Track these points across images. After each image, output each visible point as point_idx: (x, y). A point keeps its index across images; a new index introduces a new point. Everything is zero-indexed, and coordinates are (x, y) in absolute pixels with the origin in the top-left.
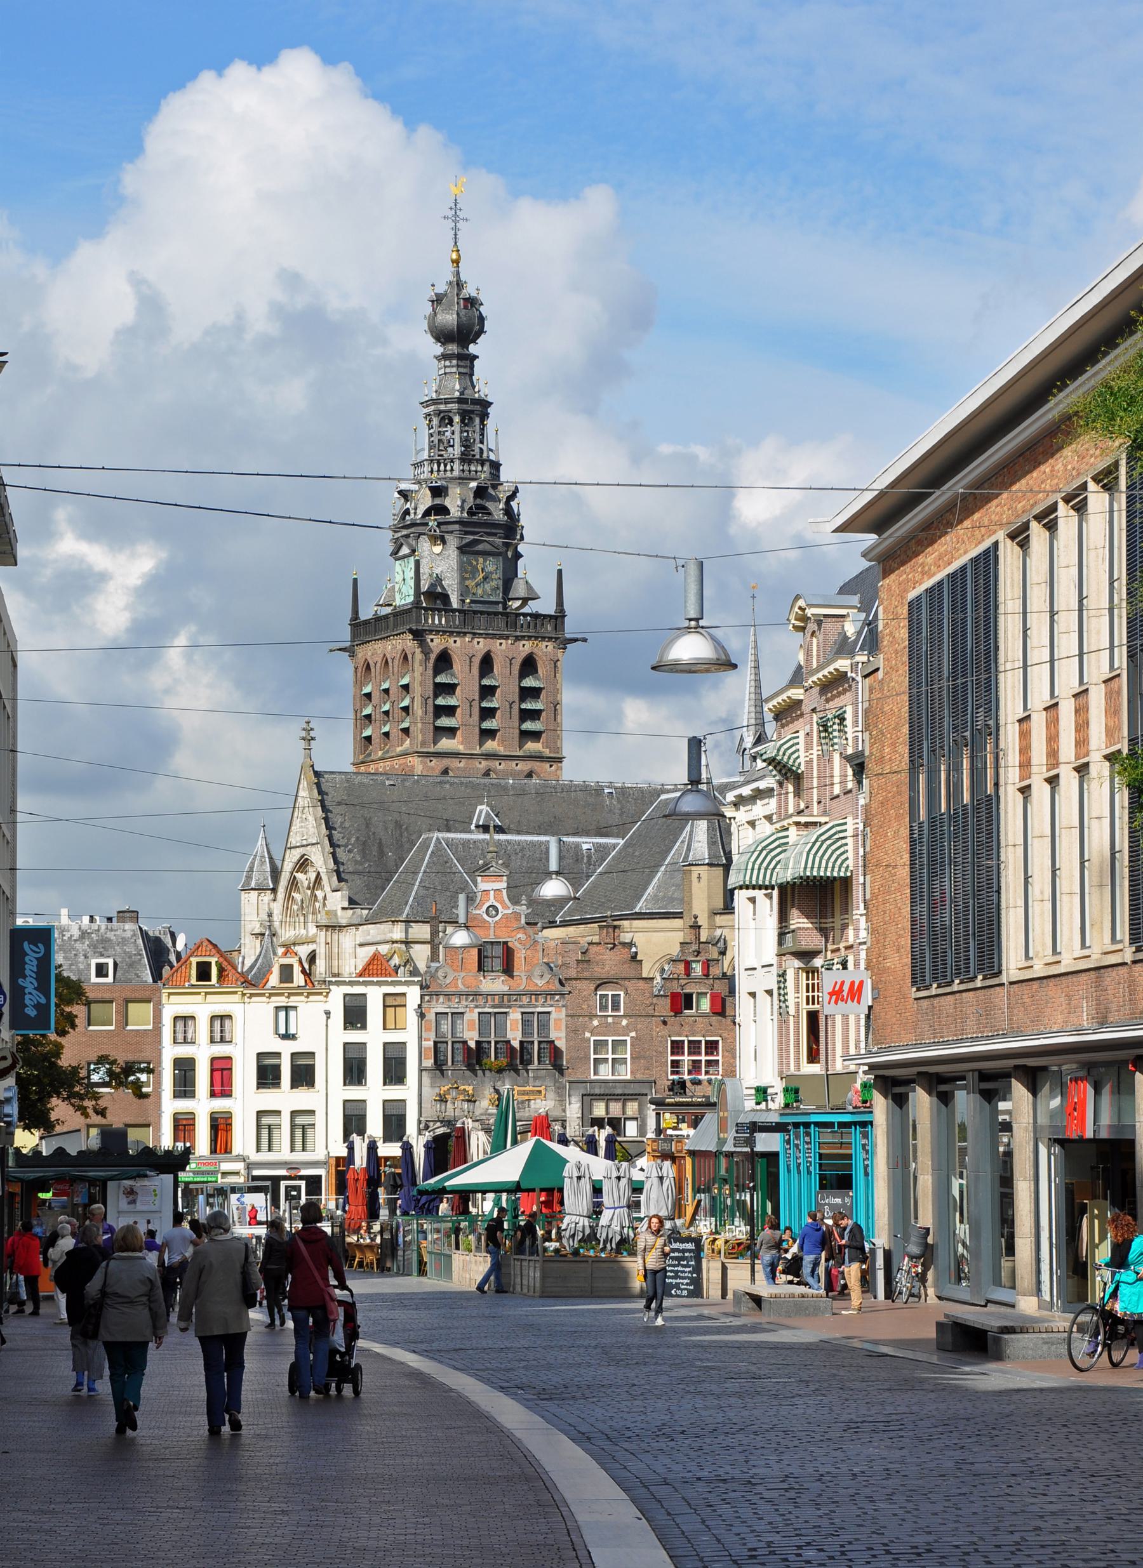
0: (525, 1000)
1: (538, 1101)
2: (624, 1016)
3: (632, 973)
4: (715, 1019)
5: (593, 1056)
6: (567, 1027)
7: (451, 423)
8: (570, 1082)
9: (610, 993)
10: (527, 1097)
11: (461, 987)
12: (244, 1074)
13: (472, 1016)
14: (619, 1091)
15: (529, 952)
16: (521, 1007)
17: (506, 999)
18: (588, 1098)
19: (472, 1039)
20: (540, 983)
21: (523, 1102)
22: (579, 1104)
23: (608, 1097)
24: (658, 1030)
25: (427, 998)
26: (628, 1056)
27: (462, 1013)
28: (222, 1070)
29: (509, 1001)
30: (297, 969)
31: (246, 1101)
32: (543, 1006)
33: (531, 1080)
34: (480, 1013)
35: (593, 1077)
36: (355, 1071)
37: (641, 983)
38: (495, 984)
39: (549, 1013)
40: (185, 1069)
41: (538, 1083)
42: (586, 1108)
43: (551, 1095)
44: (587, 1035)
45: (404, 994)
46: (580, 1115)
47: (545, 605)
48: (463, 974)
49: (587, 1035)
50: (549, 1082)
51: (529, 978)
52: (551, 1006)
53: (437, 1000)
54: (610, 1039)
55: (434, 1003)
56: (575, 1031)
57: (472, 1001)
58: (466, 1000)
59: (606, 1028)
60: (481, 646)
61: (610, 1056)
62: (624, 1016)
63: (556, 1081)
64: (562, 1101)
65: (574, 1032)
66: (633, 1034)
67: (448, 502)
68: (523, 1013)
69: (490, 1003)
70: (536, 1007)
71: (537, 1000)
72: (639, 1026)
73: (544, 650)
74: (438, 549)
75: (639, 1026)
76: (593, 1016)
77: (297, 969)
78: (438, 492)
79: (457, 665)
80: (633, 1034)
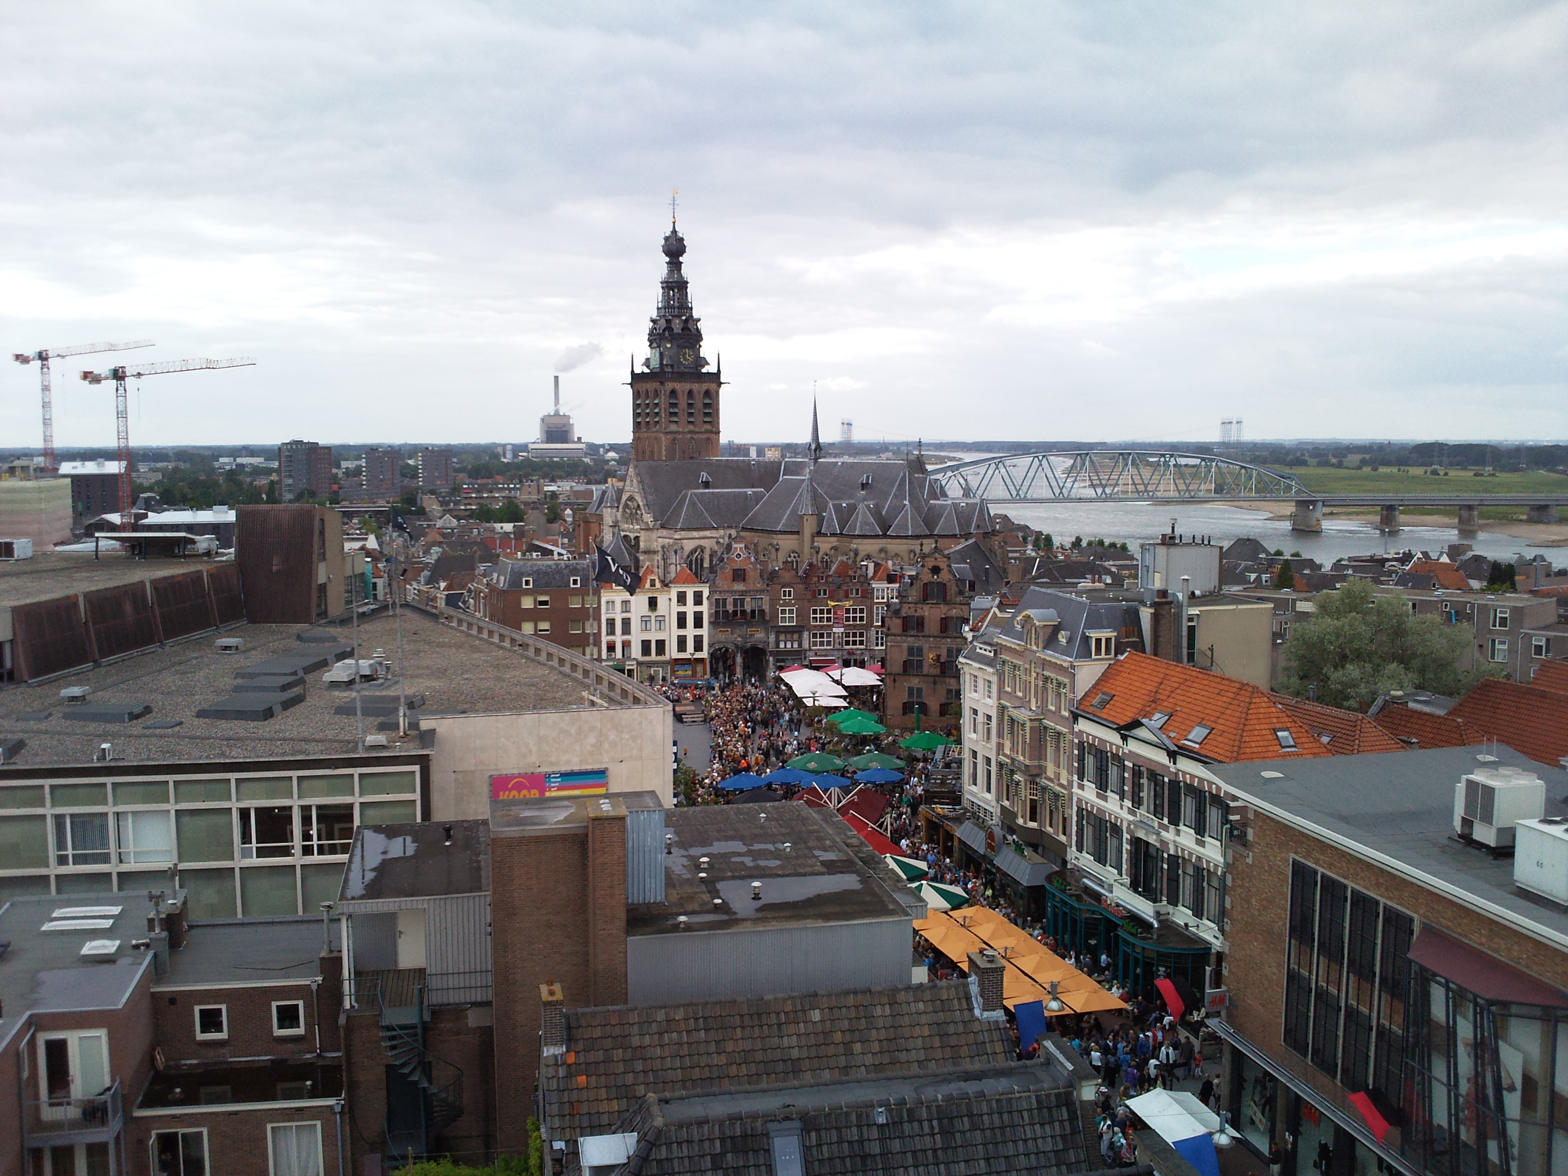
12: (635, 625)
13: (730, 600)
17: (743, 593)
23: (785, 632)
28: (626, 623)
30: (657, 581)
31: (636, 638)
36: (682, 622)
38: (739, 587)
40: (611, 623)
47: (711, 368)
60: (687, 386)
65: (773, 606)
73: (713, 386)
77: (657, 581)
78: (668, 321)
79: (680, 395)
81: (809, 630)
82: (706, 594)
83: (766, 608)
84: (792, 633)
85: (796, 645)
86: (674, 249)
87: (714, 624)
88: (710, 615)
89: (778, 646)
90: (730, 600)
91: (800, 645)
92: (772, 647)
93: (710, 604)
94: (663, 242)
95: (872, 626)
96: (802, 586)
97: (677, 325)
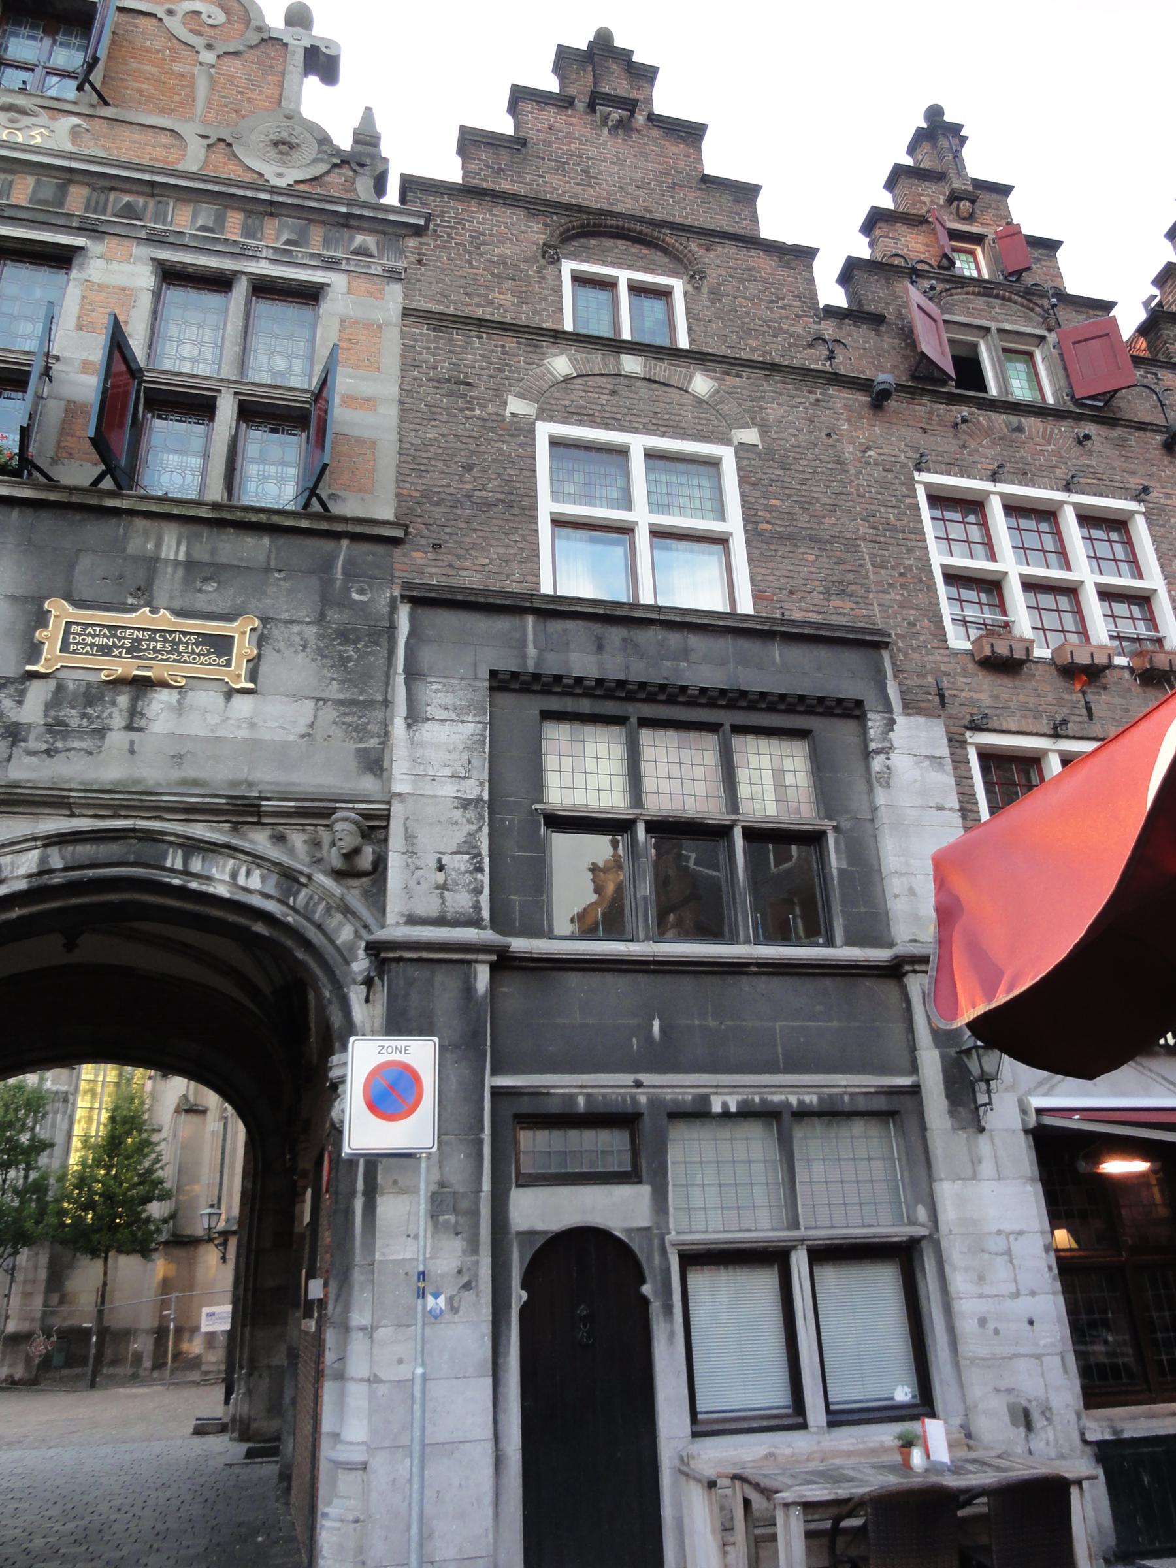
1: (206, 699)
5: (546, 507)
6: (408, 362)
8: (423, 600)
9: (624, 276)
15: (233, 66)
21: (94, 695)
22: (468, 729)
26: (734, 524)
32: (283, 256)
33: (168, 583)
41: (210, 596)
43: (295, 667)
46: (475, 789)
52: (331, 264)
54: (637, 443)
61: (642, 516)
62: (698, 358)
66: (750, 436)
70: (243, 253)
72: (774, 412)
80: (750, 436)
81: (934, 701)
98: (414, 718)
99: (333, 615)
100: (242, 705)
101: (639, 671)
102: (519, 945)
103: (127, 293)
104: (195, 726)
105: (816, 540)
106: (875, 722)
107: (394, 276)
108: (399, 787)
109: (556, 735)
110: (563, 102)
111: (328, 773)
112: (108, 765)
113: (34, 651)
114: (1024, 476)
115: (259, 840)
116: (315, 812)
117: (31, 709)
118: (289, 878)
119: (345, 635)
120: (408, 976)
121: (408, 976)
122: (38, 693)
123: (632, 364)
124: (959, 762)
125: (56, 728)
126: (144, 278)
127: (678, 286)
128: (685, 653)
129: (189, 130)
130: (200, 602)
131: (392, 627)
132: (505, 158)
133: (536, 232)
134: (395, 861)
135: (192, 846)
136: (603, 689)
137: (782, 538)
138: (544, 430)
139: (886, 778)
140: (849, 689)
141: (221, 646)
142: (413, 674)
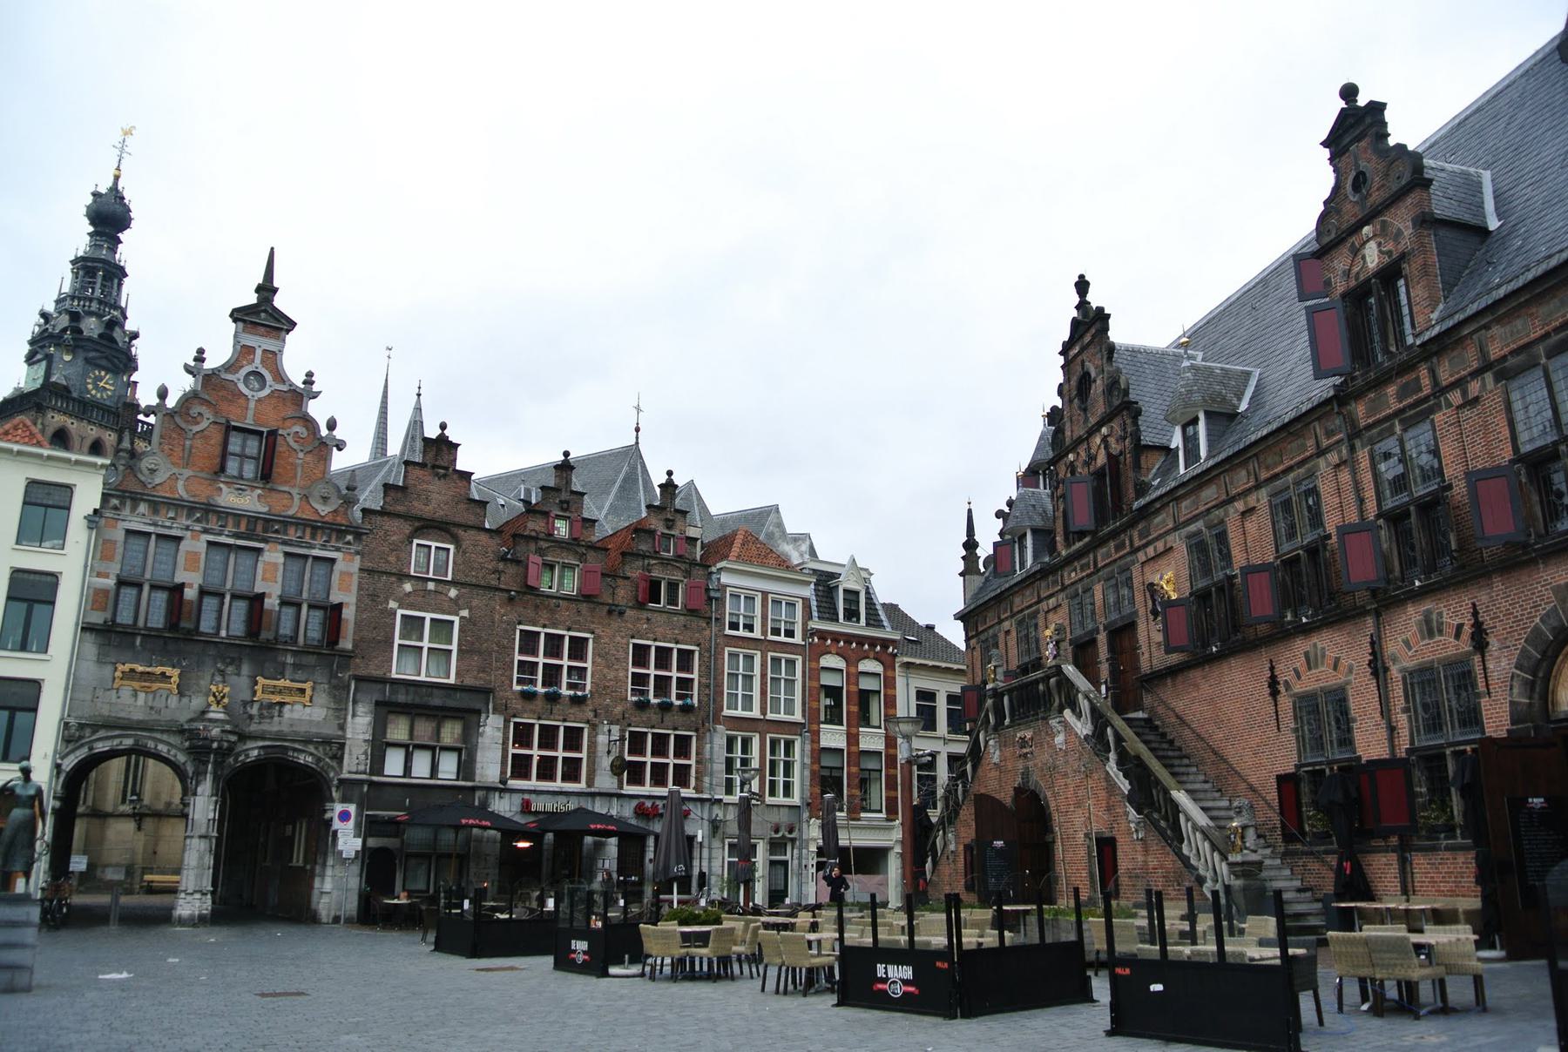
0: (292, 534)
1: (298, 707)
2: (453, 583)
3: (471, 519)
4: (584, 607)
5: (397, 641)
6: (360, 588)
7: (94, 276)
8: (359, 679)
9: (434, 544)
10: (277, 698)
11: (181, 491)
13: (195, 544)
14: (437, 702)
15: (309, 458)
16: (285, 543)
17: (260, 528)
18: (385, 710)
19: (191, 586)
20: (324, 510)
21: (271, 706)
24: (501, 612)
25: (115, 502)
26: (454, 647)
27: (178, 539)
29: (265, 530)
32: (323, 547)
33: (288, 673)
34: (210, 543)
35: (394, 675)
37: (483, 537)
39: (333, 561)
41: (300, 675)
42: (379, 727)
43: (322, 698)
44: (392, 604)
45: (68, 489)
46: (368, 737)
48: (188, 473)
49: (392, 604)
50: (320, 676)
51: (305, 498)
52: (338, 549)
53: (134, 509)
54: (428, 616)
55: (127, 511)
56: (373, 596)
57: (198, 520)
58: (189, 517)
59: (422, 598)
61: (426, 644)
62: (453, 583)
63: (333, 675)
64: (340, 713)
65: (371, 599)
66: (465, 613)
67: (83, 326)
68: (287, 554)
69: (230, 528)
70: (312, 547)
71: (313, 537)
72: (475, 603)
74: (67, 358)
75: (475, 603)
76: (404, 576)
78: (75, 317)
80: (465, 613)
81: (504, 710)
82: (88, 494)
83: (345, 595)
84: (440, 714)
85: (448, 767)
86: (109, 217)
87: (107, 634)
88: (95, 598)
89: (377, 764)
90: (195, 544)
91: (466, 767)
92: (354, 762)
93: (102, 551)
94: (89, 200)
95: (718, 718)
96: (492, 544)
97: (91, 327)
98: (354, 715)
99: (334, 681)
100: (308, 710)
101: (417, 700)
102: (375, 778)
103: (275, 565)
104: (296, 716)
105: (480, 653)
106: (483, 716)
107: (358, 553)
108: (349, 735)
109: (391, 717)
110: (422, 465)
111: (330, 730)
112: (273, 726)
113: (254, 693)
114: (554, 626)
115: (311, 749)
116: (326, 741)
117: (254, 711)
118: (319, 760)
119: (335, 687)
120: (349, 788)
121: (349, 788)
122: (256, 706)
123: (431, 586)
124: (506, 727)
125: (261, 716)
126: (281, 559)
127: (452, 547)
128: (431, 695)
129: (295, 492)
130: (297, 677)
131: (349, 686)
132: (399, 495)
133: (407, 528)
134: (346, 756)
135: (295, 750)
136: (405, 705)
137: (468, 652)
138: (400, 612)
139: (482, 735)
140: (478, 706)
141: (303, 691)
142: (355, 702)
